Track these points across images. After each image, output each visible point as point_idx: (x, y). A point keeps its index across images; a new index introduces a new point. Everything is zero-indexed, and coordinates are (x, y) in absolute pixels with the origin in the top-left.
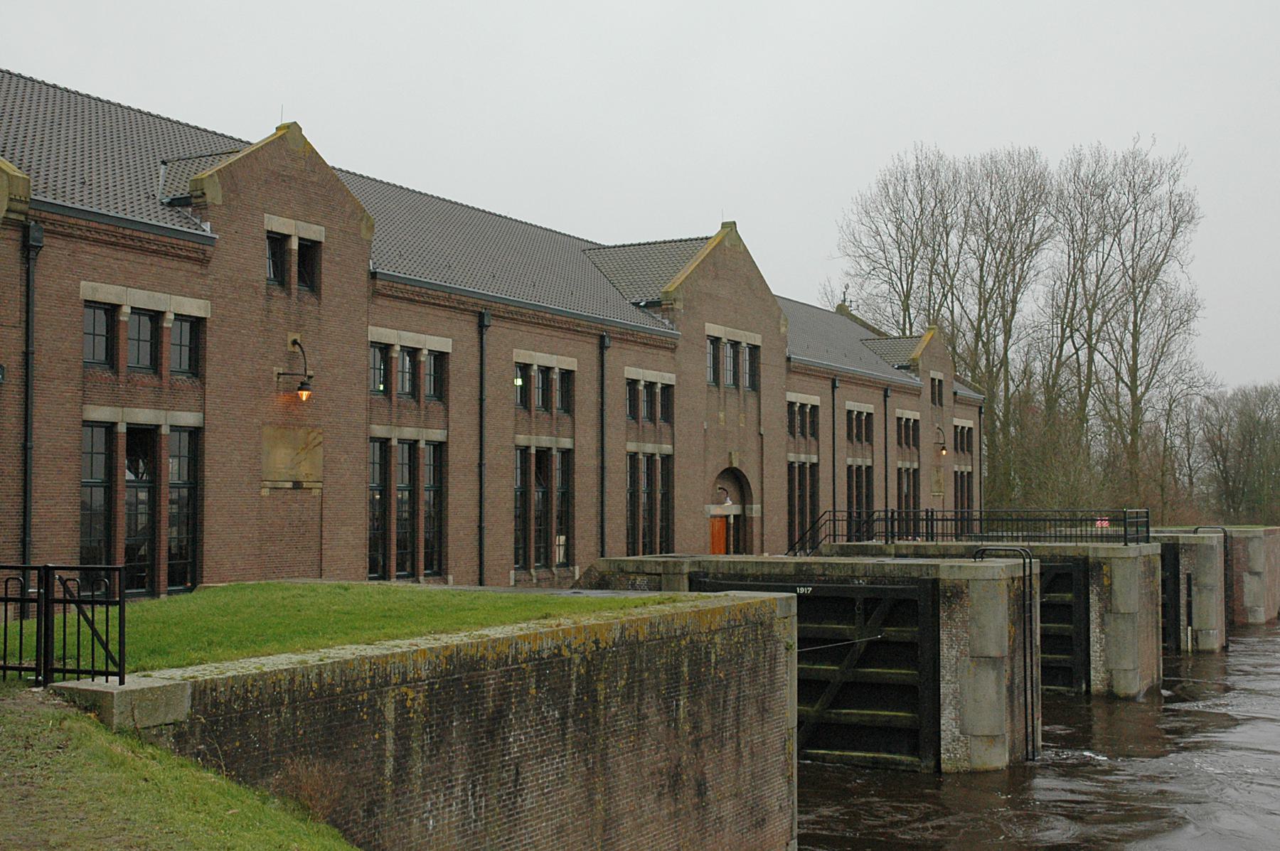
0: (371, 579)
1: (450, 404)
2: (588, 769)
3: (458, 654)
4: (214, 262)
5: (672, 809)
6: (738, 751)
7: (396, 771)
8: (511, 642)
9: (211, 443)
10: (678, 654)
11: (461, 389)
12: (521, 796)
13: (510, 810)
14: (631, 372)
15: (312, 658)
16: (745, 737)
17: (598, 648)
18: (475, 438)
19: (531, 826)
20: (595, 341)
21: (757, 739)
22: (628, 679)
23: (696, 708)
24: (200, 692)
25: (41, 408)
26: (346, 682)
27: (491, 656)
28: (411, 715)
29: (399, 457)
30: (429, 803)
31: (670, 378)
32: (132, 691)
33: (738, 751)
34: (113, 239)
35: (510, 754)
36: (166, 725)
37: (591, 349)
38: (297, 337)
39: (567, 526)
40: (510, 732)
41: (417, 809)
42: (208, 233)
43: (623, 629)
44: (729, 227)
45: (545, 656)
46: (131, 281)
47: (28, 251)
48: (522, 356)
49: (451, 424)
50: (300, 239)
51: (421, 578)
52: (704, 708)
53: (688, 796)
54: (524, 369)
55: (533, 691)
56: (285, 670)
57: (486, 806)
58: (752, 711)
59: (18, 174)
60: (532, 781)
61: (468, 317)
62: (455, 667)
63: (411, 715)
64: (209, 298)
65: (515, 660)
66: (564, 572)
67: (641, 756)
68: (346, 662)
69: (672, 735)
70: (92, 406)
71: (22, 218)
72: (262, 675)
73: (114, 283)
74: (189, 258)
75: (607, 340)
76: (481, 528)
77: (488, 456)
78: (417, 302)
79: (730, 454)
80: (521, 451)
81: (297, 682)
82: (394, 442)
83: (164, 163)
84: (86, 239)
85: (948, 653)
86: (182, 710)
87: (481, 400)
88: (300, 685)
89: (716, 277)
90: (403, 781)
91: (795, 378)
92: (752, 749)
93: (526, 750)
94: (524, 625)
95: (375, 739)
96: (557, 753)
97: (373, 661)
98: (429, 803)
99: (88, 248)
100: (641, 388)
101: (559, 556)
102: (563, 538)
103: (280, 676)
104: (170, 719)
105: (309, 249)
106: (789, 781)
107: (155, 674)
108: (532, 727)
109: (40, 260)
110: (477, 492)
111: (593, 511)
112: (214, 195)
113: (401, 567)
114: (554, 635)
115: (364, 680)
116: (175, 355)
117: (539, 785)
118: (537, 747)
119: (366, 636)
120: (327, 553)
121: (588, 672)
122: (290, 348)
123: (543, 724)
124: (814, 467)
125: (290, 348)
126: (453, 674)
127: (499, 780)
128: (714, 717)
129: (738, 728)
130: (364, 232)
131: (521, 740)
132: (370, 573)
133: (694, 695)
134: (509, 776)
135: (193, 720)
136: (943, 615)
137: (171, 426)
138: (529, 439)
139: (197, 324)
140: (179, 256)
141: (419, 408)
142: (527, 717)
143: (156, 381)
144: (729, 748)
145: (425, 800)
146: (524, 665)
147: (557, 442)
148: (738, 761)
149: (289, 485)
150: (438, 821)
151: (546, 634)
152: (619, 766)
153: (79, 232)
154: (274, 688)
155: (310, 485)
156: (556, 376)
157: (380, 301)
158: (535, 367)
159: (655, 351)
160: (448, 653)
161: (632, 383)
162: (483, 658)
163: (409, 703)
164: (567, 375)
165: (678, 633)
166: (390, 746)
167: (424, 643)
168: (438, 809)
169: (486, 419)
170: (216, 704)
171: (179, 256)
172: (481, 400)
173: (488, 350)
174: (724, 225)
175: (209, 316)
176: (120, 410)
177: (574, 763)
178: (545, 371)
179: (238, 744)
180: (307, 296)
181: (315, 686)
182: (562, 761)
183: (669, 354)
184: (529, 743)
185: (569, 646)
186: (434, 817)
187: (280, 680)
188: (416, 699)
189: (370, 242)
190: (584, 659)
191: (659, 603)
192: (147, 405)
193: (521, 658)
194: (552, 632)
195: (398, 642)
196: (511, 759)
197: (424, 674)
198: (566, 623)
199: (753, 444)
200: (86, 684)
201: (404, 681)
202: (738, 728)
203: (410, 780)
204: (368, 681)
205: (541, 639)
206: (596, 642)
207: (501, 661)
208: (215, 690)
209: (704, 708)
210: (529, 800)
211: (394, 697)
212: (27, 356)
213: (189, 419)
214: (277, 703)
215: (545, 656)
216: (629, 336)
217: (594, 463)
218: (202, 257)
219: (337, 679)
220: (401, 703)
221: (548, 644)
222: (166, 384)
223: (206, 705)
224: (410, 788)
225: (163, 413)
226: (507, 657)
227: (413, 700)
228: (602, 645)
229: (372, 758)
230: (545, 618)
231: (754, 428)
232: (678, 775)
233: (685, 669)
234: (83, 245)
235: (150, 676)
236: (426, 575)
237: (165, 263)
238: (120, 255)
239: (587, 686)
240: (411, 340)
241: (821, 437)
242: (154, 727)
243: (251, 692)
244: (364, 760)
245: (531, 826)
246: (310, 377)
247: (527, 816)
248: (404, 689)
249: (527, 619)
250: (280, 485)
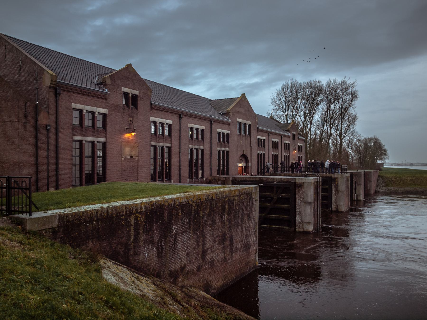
0: (151, 181)
1: (172, 137)
2: (197, 236)
3: (155, 204)
4: (108, 100)
5: (223, 246)
6: (242, 229)
7: (134, 239)
8: (173, 200)
9: (108, 146)
10: (225, 202)
11: (175, 134)
12: (176, 245)
13: (173, 249)
14: (219, 130)
15: (105, 206)
16: (244, 225)
17: (200, 201)
18: (178, 146)
19: (180, 253)
20: (209, 122)
21: (247, 225)
22: (210, 210)
23: (230, 218)
24: (62, 217)
25: (61, 136)
26: (117, 213)
27: (166, 204)
28: (140, 222)
29: (159, 150)
30: (146, 249)
31: (228, 132)
32: (34, 218)
33: (242, 229)
34: (80, 92)
35: (173, 233)
36: (49, 229)
37: (208, 124)
38: (131, 119)
39: (202, 169)
40: (173, 226)
41: (142, 250)
43: (208, 195)
44: (243, 95)
45: (184, 203)
46: (85, 104)
47: (57, 95)
48: (190, 125)
49: (172, 142)
50: (132, 94)
51: (165, 181)
52: (232, 217)
53: (228, 243)
54: (192, 129)
55: (180, 214)
56: (95, 210)
57: (165, 248)
58: (246, 218)
59: (54, 74)
60: (180, 240)
61: (176, 115)
62: (154, 207)
63: (140, 222)
65: (174, 204)
66: (202, 180)
67: (214, 231)
68: (117, 207)
69: (223, 226)
70: (75, 136)
71: (55, 86)
72: (86, 211)
73: (81, 104)
74: (101, 98)
75: (212, 122)
76: (180, 168)
77: (182, 150)
78: (163, 111)
79: (243, 151)
80: (191, 149)
81: (99, 214)
82: (157, 147)
83: (98, 75)
84: (73, 92)
85: (298, 201)
86: (56, 223)
87: (180, 136)
88: (100, 214)
89: (240, 107)
90: (137, 242)
91: (260, 133)
92: (246, 228)
93: (178, 231)
94: (178, 195)
95: (127, 230)
96: (188, 232)
97: (127, 206)
98: (146, 249)
99: (74, 95)
100: (221, 134)
101: (200, 175)
102: (201, 171)
103: (92, 212)
104: (49, 227)
105: (135, 97)
106: (256, 237)
107: (49, 212)
108: (180, 224)
109: (60, 97)
110: (179, 159)
111: (209, 164)
112: (109, 82)
113: (159, 178)
114: (186, 197)
115: (123, 212)
116: (99, 124)
117: (182, 241)
118: (181, 230)
119: (128, 198)
120: (140, 175)
121: (197, 208)
122: (130, 122)
123: (183, 224)
124: (264, 154)
125: (130, 122)
126: (154, 210)
127: (169, 240)
128: (235, 220)
129: (242, 223)
130: (149, 93)
131: (176, 228)
132: (151, 180)
133: (229, 214)
134: (173, 239)
135: (59, 227)
136: (297, 191)
137: (97, 142)
138: (192, 147)
139: (104, 115)
140: (99, 98)
141: (164, 138)
142: (178, 222)
143: (93, 130)
144: (239, 228)
145: (144, 248)
146: (177, 207)
147: (200, 147)
148: (242, 232)
149: (129, 157)
150: (149, 254)
151: (184, 197)
152: (207, 234)
153: (71, 90)
154: (91, 215)
155: (135, 157)
156: (200, 131)
158: (194, 128)
159: (225, 125)
160: (152, 203)
161: (219, 133)
162: (164, 205)
163: (139, 219)
164: (202, 131)
165: (225, 196)
166: (132, 232)
167: (144, 200)
168: (149, 250)
169: (181, 141)
170: (68, 221)
171: (99, 98)
172: (180, 136)
173: (182, 124)
174: (242, 94)
175: (107, 113)
176: (83, 137)
177: (193, 235)
178: (197, 129)
179: (77, 234)
180: (136, 110)
181: (105, 214)
182: (189, 234)
183: (228, 126)
184: (179, 229)
185: (191, 201)
186: (147, 253)
187: (93, 213)
188: (142, 218)
189: (151, 95)
190: (196, 204)
191: (220, 188)
192: (90, 136)
193: (176, 204)
194: (186, 197)
195: (136, 200)
196: (173, 234)
197: (144, 210)
198: (191, 194)
199: (249, 149)
200: (20, 216)
201: (137, 212)
202: (242, 223)
203: (140, 242)
204: (125, 212)
205: (183, 199)
206: (200, 199)
207: (169, 205)
208: (68, 217)
209: (232, 217)
210: (179, 246)
211: (134, 217)
212: (57, 122)
213: (102, 140)
214: (91, 221)
215: (184, 203)
216: (217, 121)
217: (209, 152)
218: (105, 98)
219: (114, 213)
220: (136, 219)
221: (185, 200)
222: (96, 130)
223: (64, 222)
224: (140, 244)
226: (172, 204)
227: (140, 218)
228: (202, 200)
229: (126, 236)
230: (185, 192)
231: (249, 145)
232: (225, 236)
233: (227, 207)
234: (72, 94)
235: (46, 212)
236: (166, 180)
237: (95, 99)
238: (83, 97)
239: (197, 212)
240: (161, 120)
241: (266, 146)
242: (44, 230)
243: (82, 217)
244: (124, 236)
245: (180, 253)
246: (135, 130)
247: (178, 251)
248: (137, 215)
249: (180, 193)
250: (127, 157)
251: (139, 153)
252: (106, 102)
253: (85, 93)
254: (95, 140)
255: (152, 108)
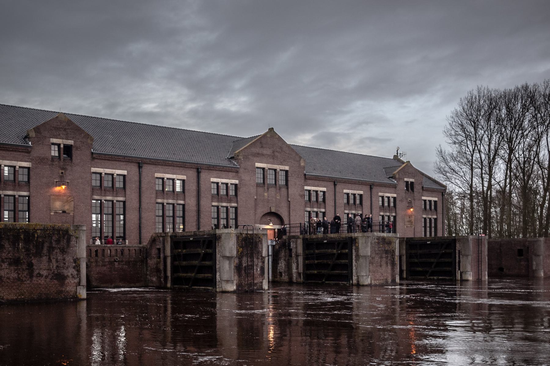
1: (126, 190)
11: (132, 187)
18: (137, 200)
42: (31, 145)
49: (127, 196)
50: (64, 144)
64: (30, 162)
77: (144, 205)
78: (111, 160)
110: (138, 216)
140: (20, 151)
157: (96, 161)
169: (143, 195)
175: (31, 166)
225: (16, 192)
250: (58, 212)
251: (74, 207)
252: (29, 155)
253: (3, 149)
254: (16, 194)
255: (93, 158)
